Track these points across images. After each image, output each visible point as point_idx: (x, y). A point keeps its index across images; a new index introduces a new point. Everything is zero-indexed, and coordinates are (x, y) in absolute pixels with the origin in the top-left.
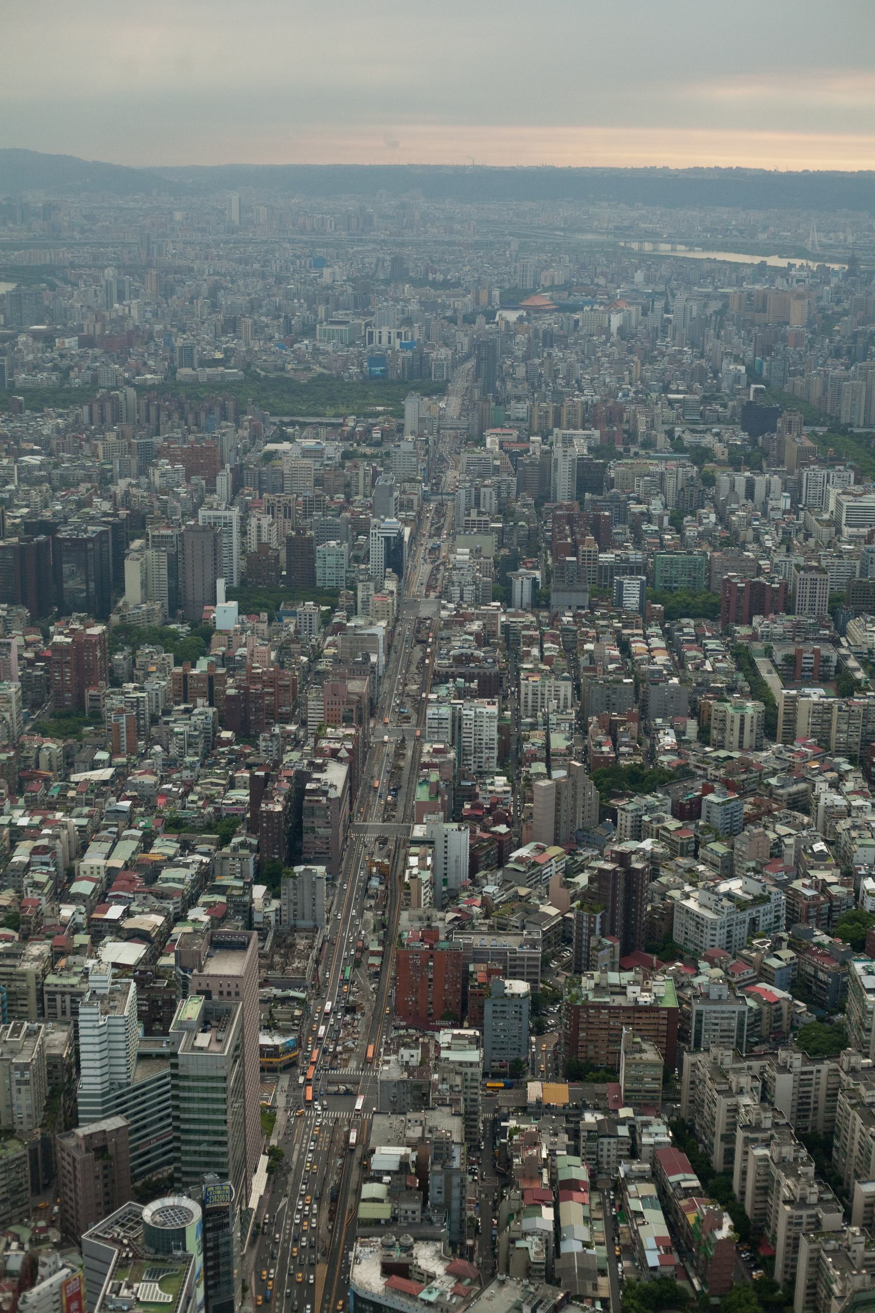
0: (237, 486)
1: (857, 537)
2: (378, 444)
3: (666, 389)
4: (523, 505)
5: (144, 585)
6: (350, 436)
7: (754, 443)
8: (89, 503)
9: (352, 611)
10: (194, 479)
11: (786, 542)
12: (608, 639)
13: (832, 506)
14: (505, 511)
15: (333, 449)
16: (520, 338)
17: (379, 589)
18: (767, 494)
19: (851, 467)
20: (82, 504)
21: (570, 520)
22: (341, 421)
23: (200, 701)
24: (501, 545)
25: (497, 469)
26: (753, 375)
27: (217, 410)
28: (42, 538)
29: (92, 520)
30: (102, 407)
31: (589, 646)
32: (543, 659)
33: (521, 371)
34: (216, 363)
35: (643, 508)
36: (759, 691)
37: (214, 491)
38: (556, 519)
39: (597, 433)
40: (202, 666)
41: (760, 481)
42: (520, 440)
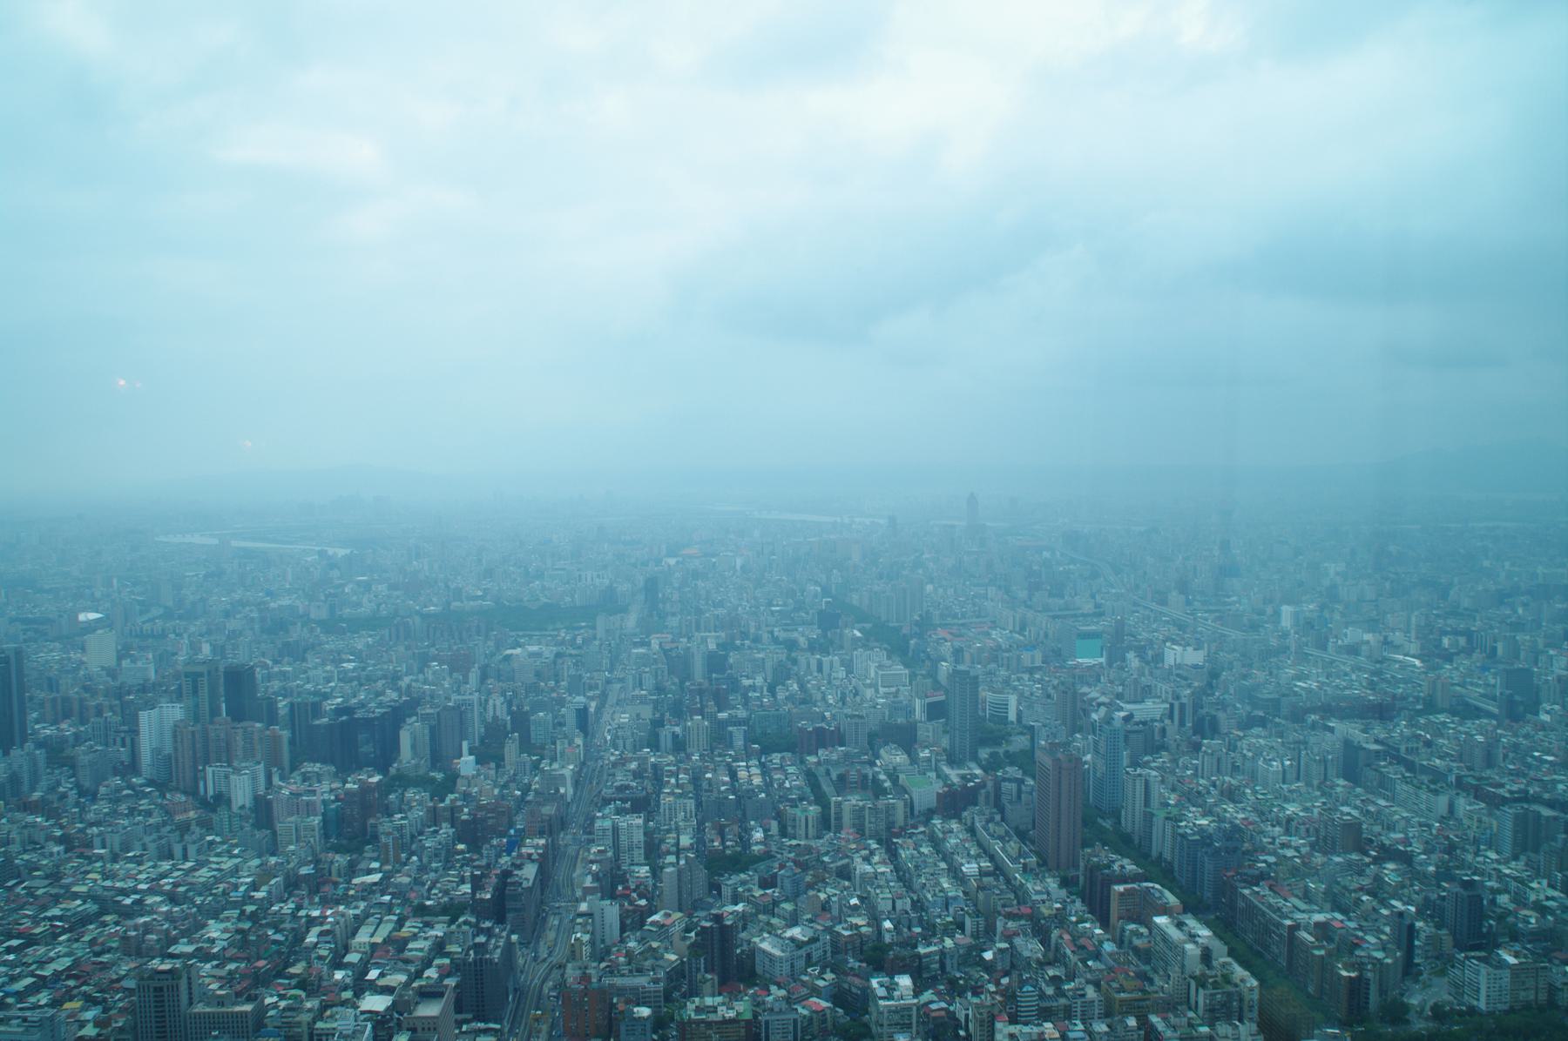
0: (484, 678)
2: (579, 648)
3: (770, 604)
4: (671, 683)
5: (414, 747)
6: (562, 643)
7: (825, 636)
8: (383, 693)
9: (554, 759)
10: (455, 675)
11: (843, 700)
12: (722, 770)
14: (659, 689)
15: (549, 652)
16: (677, 575)
20: (378, 694)
21: (701, 692)
24: (655, 708)
25: (655, 661)
29: (380, 705)
31: (709, 775)
32: (678, 786)
33: (676, 597)
34: (476, 598)
36: (821, 799)
40: (448, 801)
42: (673, 641)
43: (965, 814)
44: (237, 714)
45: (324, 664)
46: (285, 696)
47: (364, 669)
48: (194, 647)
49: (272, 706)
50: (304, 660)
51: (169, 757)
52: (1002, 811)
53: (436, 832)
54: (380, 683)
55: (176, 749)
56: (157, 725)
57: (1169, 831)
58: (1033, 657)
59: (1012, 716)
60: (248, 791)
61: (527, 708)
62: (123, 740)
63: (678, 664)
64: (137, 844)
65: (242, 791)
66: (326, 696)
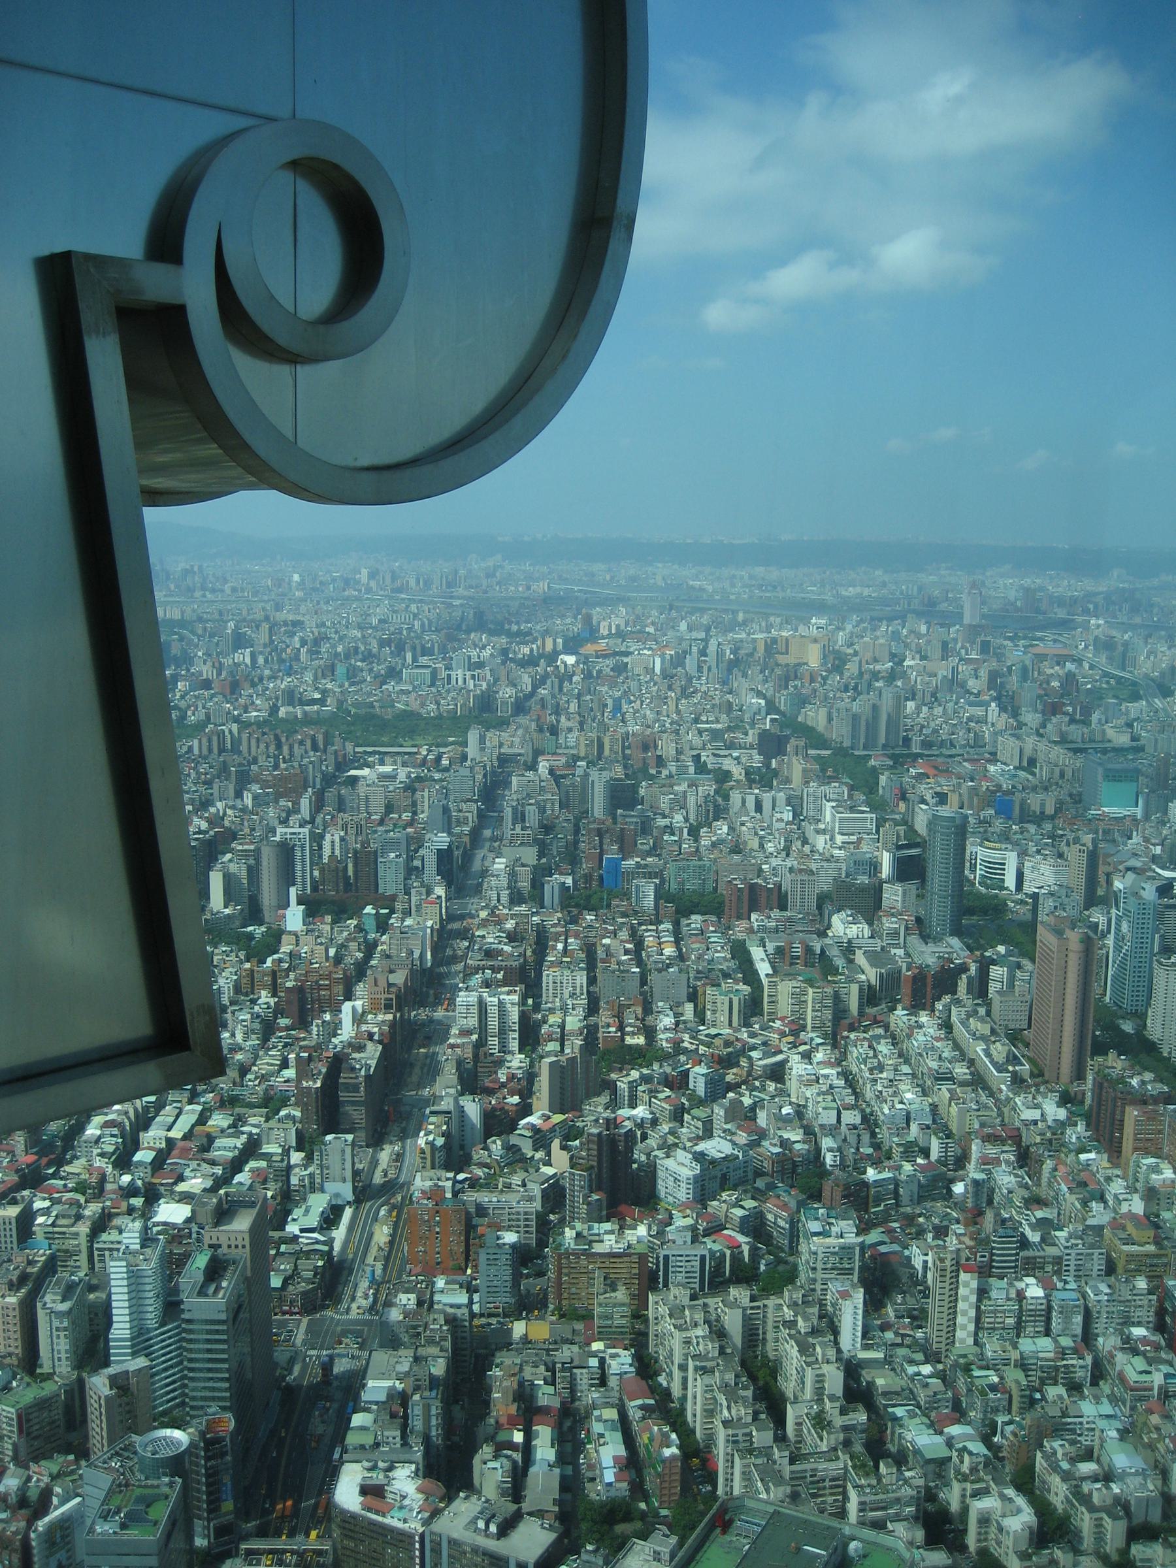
0: (318, 805)
1: (848, 843)
3: (697, 720)
4: (564, 820)
7: (767, 765)
9: (407, 913)
10: (282, 802)
12: (624, 934)
13: (828, 818)
17: (429, 892)
19: (846, 784)
21: (600, 833)
22: (415, 750)
23: (263, 993)
24: (541, 855)
26: (771, 707)
27: (309, 743)
30: (210, 741)
31: (606, 941)
32: (565, 951)
34: (313, 702)
35: (666, 822)
37: (296, 810)
38: (589, 831)
41: (767, 798)
52: (988, 1004)
53: (253, 1002)
58: (1043, 805)
59: (1010, 881)
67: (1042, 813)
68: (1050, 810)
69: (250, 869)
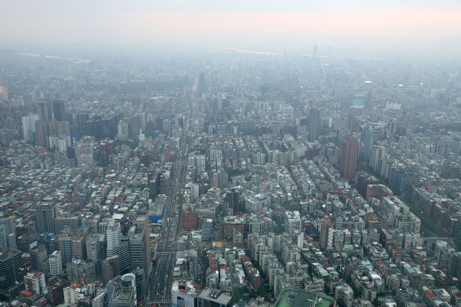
0: (145, 107)
3: (243, 83)
6: (171, 95)
8: (109, 112)
9: (171, 136)
10: (134, 106)
12: (230, 140)
13: (281, 109)
15: (167, 99)
17: (177, 130)
18: (266, 106)
21: (221, 114)
23: (136, 157)
24: (206, 119)
28: (98, 120)
29: (110, 116)
31: (226, 142)
32: (215, 145)
34: (139, 79)
35: (238, 110)
36: (264, 151)
37: (139, 108)
38: (218, 113)
39: (227, 94)
40: (136, 149)
42: (210, 95)
43: (315, 158)
44: (59, 118)
45: (87, 101)
46: (74, 112)
47: (101, 103)
48: (38, 94)
49: (70, 116)
50: (79, 100)
51: (35, 133)
54: (108, 108)
55: (37, 130)
56: (29, 122)
57: (388, 167)
58: (337, 105)
59: (330, 125)
60: (65, 145)
61: (161, 118)
62: (16, 127)
63: (214, 104)
64: (27, 163)
65: (63, 145)
66: (90, 112)
67: (337, 107)
68: (339, 107)
69: (129, 125)
